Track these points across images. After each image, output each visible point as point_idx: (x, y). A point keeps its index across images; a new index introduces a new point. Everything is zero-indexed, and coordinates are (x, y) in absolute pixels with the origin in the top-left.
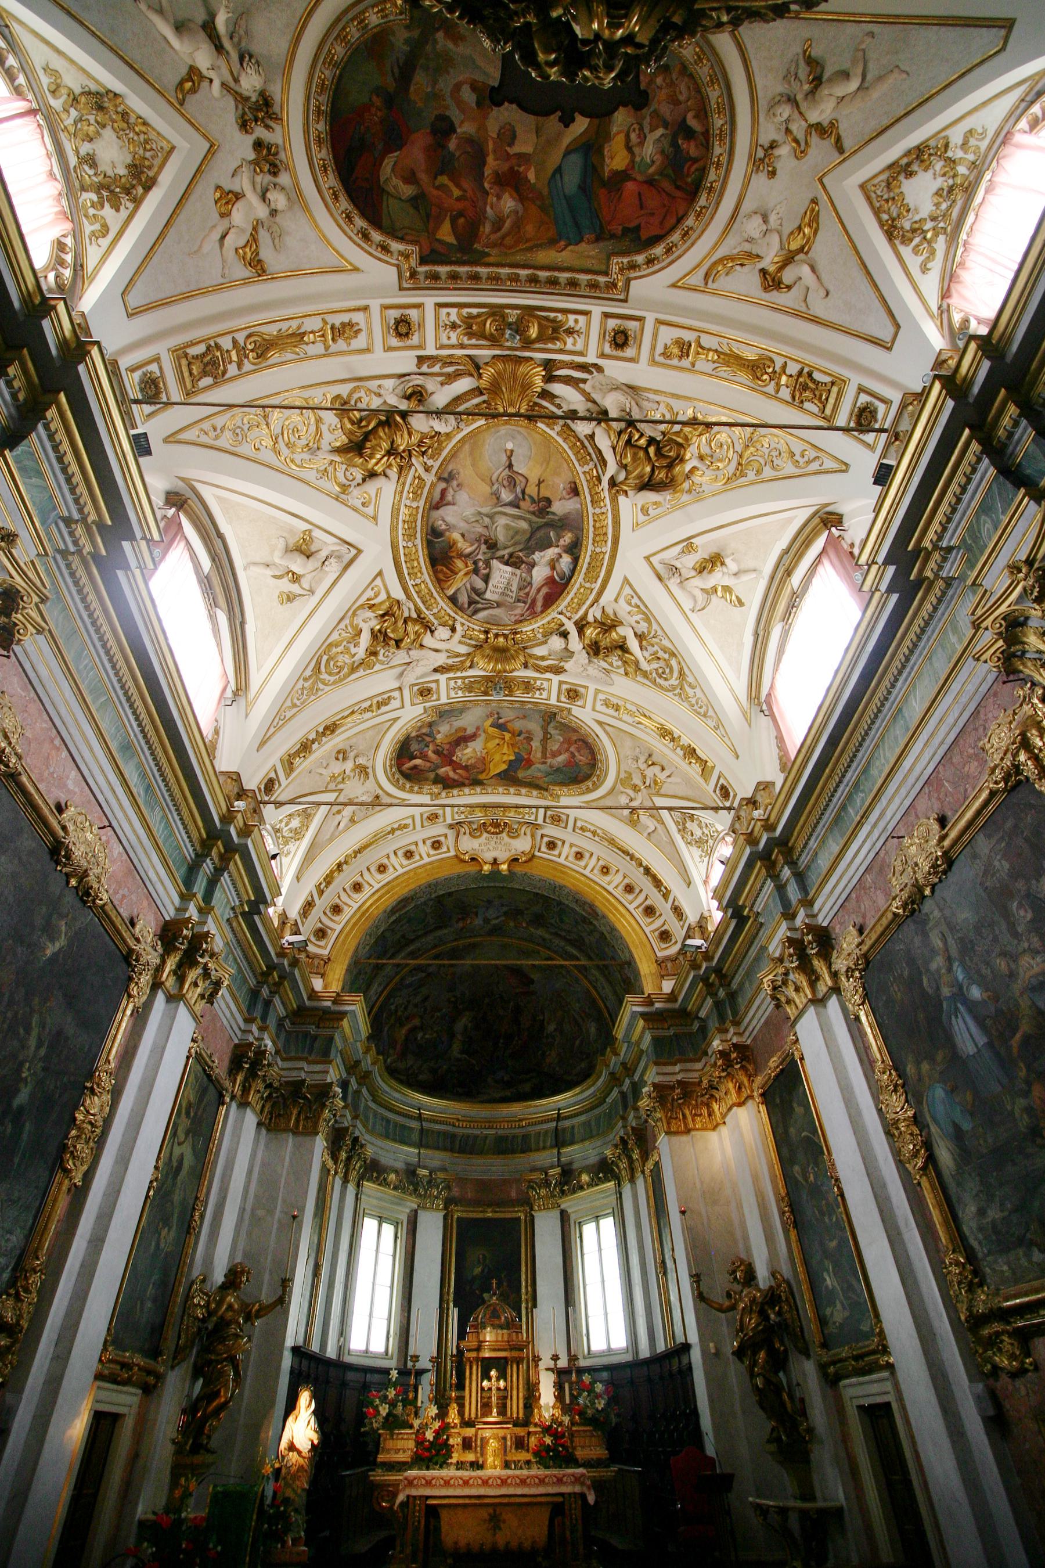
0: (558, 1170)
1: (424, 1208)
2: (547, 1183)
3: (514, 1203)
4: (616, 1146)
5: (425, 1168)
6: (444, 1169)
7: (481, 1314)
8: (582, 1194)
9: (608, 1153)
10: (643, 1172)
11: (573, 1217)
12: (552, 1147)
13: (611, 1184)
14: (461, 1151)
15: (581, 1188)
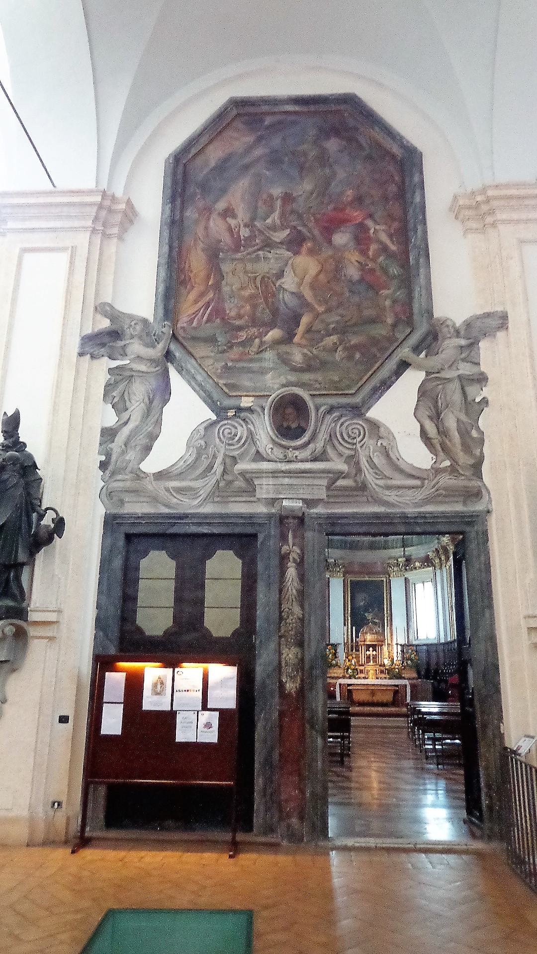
0: (404, 559)
1: (333, 577)
2: (398, 565)
3: (379, 573)
4: (433, 552)
5: (332, 558)
6: (341, 558)
7: (365, 629)
8: (415, 572)
9: (430, 554)
10: (446, 566)
11: (411, 581)
12: (400, 547)
13: (431, 569)
14: (350, 549)
15: (415, 568)
